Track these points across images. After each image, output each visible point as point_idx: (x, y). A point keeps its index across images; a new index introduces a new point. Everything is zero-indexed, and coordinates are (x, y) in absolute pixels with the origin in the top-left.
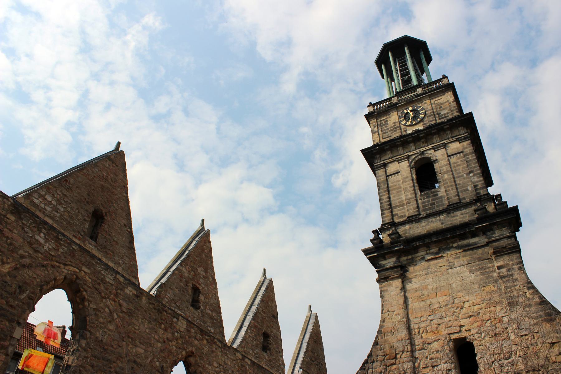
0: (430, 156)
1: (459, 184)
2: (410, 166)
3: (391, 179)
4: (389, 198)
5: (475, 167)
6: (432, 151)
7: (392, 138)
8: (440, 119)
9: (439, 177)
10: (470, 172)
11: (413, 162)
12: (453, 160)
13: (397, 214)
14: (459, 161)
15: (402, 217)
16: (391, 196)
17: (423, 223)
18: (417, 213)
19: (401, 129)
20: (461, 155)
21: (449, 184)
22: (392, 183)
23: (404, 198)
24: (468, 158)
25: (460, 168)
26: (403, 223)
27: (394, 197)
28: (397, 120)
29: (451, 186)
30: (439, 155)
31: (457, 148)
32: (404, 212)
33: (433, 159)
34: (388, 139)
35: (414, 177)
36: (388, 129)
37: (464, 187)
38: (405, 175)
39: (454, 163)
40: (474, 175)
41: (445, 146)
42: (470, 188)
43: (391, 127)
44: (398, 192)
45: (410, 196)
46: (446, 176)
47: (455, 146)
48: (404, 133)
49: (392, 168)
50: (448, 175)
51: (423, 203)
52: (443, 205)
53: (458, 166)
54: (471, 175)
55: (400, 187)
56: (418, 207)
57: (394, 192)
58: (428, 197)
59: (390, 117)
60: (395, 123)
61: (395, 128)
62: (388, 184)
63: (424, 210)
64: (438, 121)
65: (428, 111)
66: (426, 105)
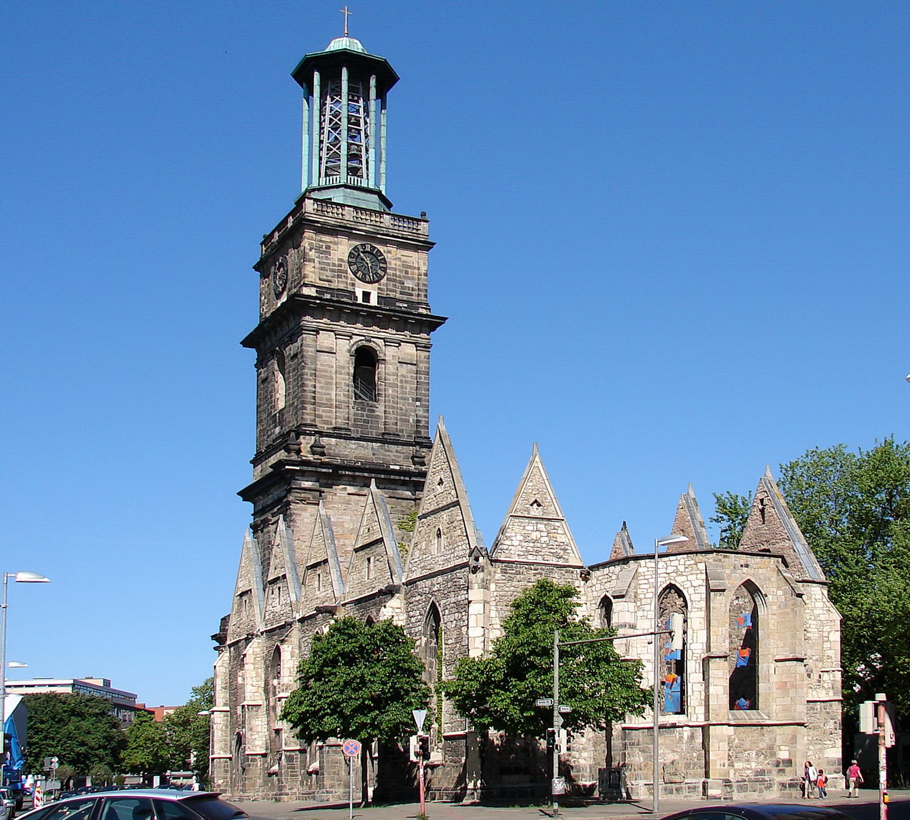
0: (378, 348)
1: (401, 409)
2: (349, 351)
3: (323, 356)
4: (315, 387)
5: (425, 395)
6: (381, 342)
7: (334, 285)
8: (401, 293)
9: (381, 386)
10: (417, 400)
11: (355, 347)
12: (404, 370)
13: (321, 416)
14: (409, 375)
15: (327, 422)
16: (317, 385)
17: (353, 444)
18: (346, 426)
19: (346, 278)
20: (414, 368)
21: (391, 404)
22: (321, 365)
23: (334, 397)
24: (420, 378)
25: (408, 386)
26: (329, 435)
27: (321, 388)
28: (346, 259)
29: (393, 408)
30: (389, 353)
31: (411, 355)
32: (330, 417)
33: (381, 356)
34: (326, 284)
35: (352, 371)
36: (328, 264)
37: (405, 415)
38: (342, 363)
39: (402, 376)
40: (421, 406)
41: (399, 343)
42: (411, 421)
43: (334, 265)
44: (327, 383)
45: (342, 398)
46: (390, 391)
47: (409, 350)
48: (350, 288)
49: (326, 340)
50: (393, 391)
51: (355, 414)
52: (378, 428)
53: (406, 382)
54: (418, 404)
55: (331, 378)
56: (348, 419)
57: (322, 380)
58: (363, 409)
59: (336, 244)
60: (342, 260)
61: (339, 271)
62: (316, 364)
63: (355, 426)
64: (398, 296)
65: (391, 268)
66: (390, 255)
